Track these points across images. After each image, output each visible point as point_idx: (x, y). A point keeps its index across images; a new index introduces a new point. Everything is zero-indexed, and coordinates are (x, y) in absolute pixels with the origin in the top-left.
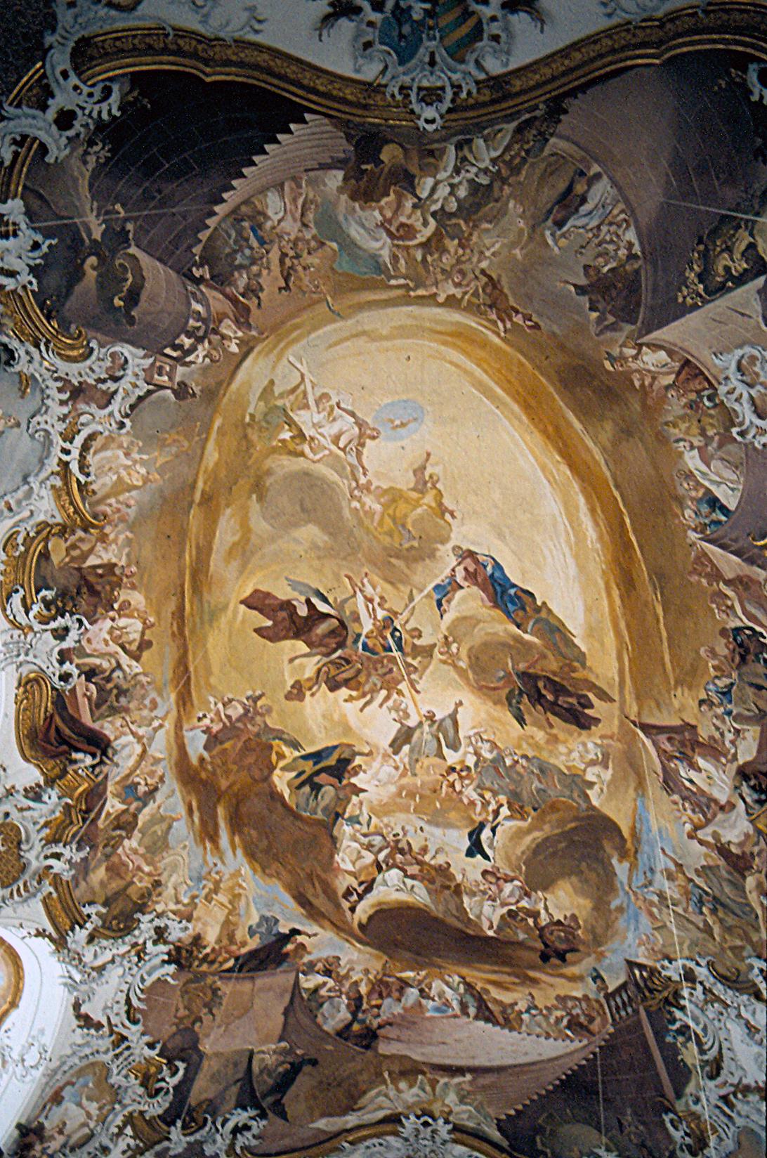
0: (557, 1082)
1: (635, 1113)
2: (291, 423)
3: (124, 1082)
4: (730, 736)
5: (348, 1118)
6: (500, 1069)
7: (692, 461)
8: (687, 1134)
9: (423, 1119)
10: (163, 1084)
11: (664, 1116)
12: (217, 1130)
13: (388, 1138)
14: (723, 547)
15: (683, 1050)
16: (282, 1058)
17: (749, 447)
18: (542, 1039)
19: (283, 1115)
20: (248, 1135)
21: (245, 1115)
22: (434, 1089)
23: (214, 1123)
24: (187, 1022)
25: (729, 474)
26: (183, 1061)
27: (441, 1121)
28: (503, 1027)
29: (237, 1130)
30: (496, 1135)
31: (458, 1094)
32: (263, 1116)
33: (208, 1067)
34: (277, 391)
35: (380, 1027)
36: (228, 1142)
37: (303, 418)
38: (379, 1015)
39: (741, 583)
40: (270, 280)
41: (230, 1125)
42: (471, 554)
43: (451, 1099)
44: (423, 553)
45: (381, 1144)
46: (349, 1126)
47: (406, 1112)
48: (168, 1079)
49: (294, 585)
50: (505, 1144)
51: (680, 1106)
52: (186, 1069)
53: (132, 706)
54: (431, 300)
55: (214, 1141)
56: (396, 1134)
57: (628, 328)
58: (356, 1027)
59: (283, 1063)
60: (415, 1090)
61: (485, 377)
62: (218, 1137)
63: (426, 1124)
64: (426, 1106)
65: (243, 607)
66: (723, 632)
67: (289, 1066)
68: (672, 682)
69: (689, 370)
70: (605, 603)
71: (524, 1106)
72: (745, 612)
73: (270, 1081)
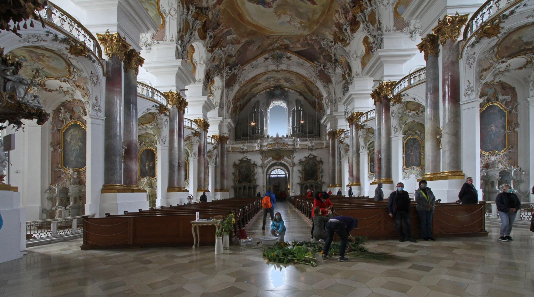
2: (302, 26)
4: (214, 11)
7: (235, 36)
14: (227, 32)
17: (228, 44)
25: (229, 39)
34: (303, 30)
37: (299, 25)
39: (222, 30)
40: (301, 41)
42: (270, 7)
44: (279, 6)
49: (306, 3)
53: (343, 4)
54: (277, 36)
57: (248, 41)
61: (269, 29)
65: (317, 4)
66: (222, 23)
68: (227, 8)
69: (239, 43)
70: (242, 9)
72: (221, 29)
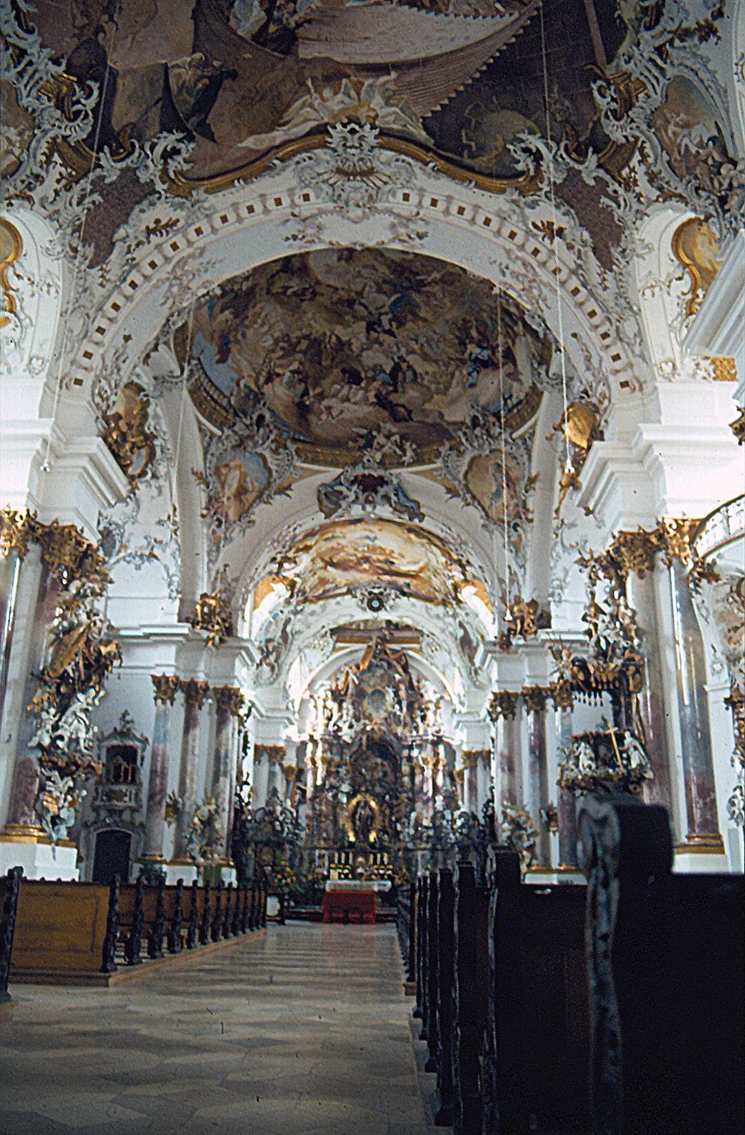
0: (484, 68)
1: (562, 89)
3: (36, 104)
5: (275, 133)
6: (426, 62)
8: (613, 100)
9: (349, 127)
10: (79, 107)
11: (592, 85)
12: (147, 156)
13: (316, 151)
15: (622, 3)
16: (199, 72)
18: (470, 19)
19: (210, 136)
20: (179, 158)
21: (172, 137)
22: (358, 94)
23: (142, 148)
24: (89, 33)
26: (96, 80)
27: (367, 127)
28: (429, 10)
29: (167, 155)
30: (422, 135)
31: (383, 96)
32: (190, 138)
33: (125, 86)
35: (298, 25)
36: (160, 167)
38: (295, 12)
41: (159, 150)
43: (377, 101)
45: (310, 158)
46: (278, 142)
47: (333, 122)
48: (83, 101)
50: (431, 142)
51: (610, 71)
52: (100, 89)
55: (147, 167)
56: (324, 145)
58: (272, 28)
59: (203, 77)
60: (340, 97)
62: (149, 163)
63: (353, 131)
64: (351, 112)
67: (206, 81)
71: (450, 99)
73: (192, 101)
